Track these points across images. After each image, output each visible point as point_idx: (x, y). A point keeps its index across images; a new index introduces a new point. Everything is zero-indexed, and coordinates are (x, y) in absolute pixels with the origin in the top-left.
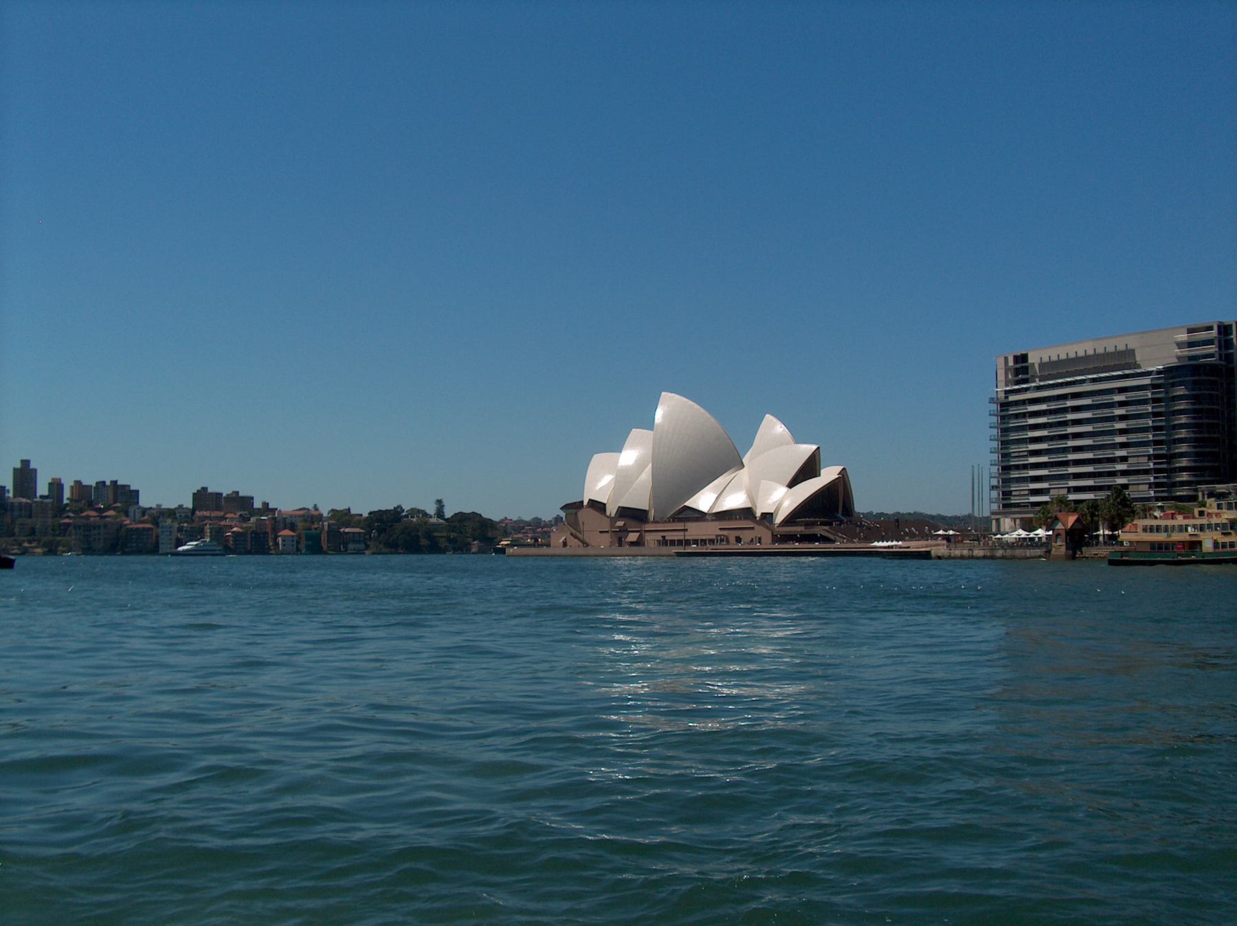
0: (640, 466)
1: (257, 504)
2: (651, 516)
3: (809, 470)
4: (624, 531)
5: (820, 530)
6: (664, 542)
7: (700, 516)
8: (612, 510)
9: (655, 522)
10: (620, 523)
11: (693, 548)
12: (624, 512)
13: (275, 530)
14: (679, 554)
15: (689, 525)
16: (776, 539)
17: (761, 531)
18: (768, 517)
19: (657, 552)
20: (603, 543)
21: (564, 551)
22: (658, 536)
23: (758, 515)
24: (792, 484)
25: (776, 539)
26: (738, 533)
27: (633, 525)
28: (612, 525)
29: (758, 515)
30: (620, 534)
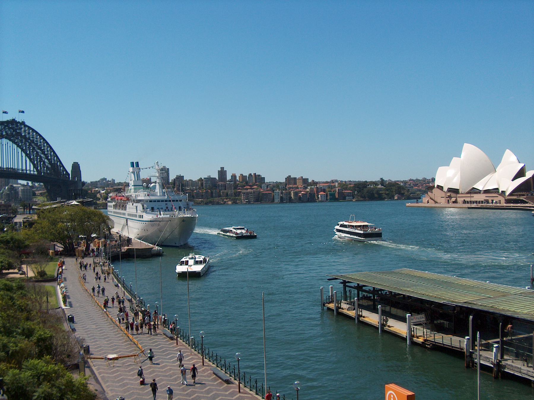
0: (455, 175)
1: (310, 181)
3: (521, 173)
4: (450, 197)
5: (522, 198)
6: (465, 202)
7: (478, 192)
8: (445, 189)
9: (462, 194)
10: (449, 194)
11: (474, 205)
13: (318, 192)
14: (469, 208)
15: (475, 195)
17: (501, 198)
18: (503, 192)
19: (461, 206)
20: (442, 202)
22: (462, 199)
23: (500, 191)
24: (513, 180)
25: (508, 201)
26: (492, 198)
27: (453, 195)
28: (446, 195)
29: (500, 191)
30: (448, 199)
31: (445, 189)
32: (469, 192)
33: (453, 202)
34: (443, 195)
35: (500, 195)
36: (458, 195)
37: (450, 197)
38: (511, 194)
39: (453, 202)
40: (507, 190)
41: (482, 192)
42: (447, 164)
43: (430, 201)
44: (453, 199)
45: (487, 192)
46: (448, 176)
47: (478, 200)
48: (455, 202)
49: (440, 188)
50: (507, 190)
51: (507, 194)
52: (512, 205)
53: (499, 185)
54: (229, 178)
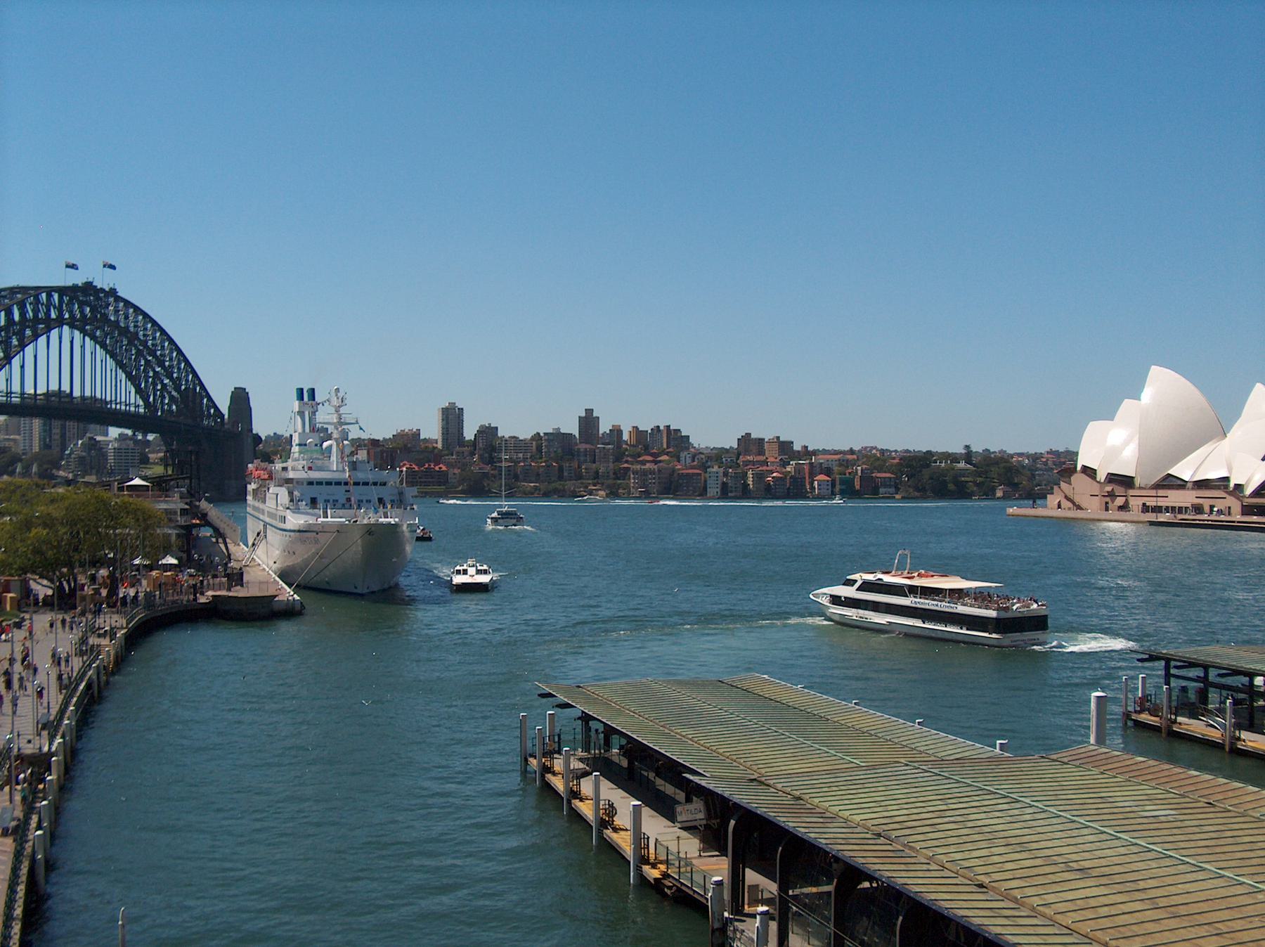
0: (1127, 443)
1: (797, 447)
2: (1137, 482)
4: (1112, 495)
6: (1146, 509)
7: (1180, 484)
8: (1101, 476)
9: (1140, 488)
10: (1109, 488)
11: (1163, 517)
12: (1113, 478)
13: (812, 475)
14: (1152, 523)
16: (1247, 510)
18: (1239, 487)
19: (1135, 519)
20: (1093, 507)
21: (1059, 513)
22: (1140, 501)
23: (1232, 485)
25: (1247, 510)
26: (1212, 502)
29: (1232, 485)
30: (1108, 499)
31: (1101, 476)
32: (1158, 486)
33: (1121, 508)
34: (1095, 489)
35: (1230, 493)
36: (1131, 492)
37: (1112, 495)
38: (1257, 493)
39: (1121, 508)
40: (1248, 481)
41: (1189, 485)
42: (1110, 416)
43: (1065, 504)
44: (1120, 501)
45: (1202, 484)
46: (1110, 445)
47: (1177, 505)
48: (1125, 507)
49: (1089, 472)
50: (1248, 481)
51: (1248, 491)
52: (1255, 518)
53: (1230, 472)
54: (469, 433)
